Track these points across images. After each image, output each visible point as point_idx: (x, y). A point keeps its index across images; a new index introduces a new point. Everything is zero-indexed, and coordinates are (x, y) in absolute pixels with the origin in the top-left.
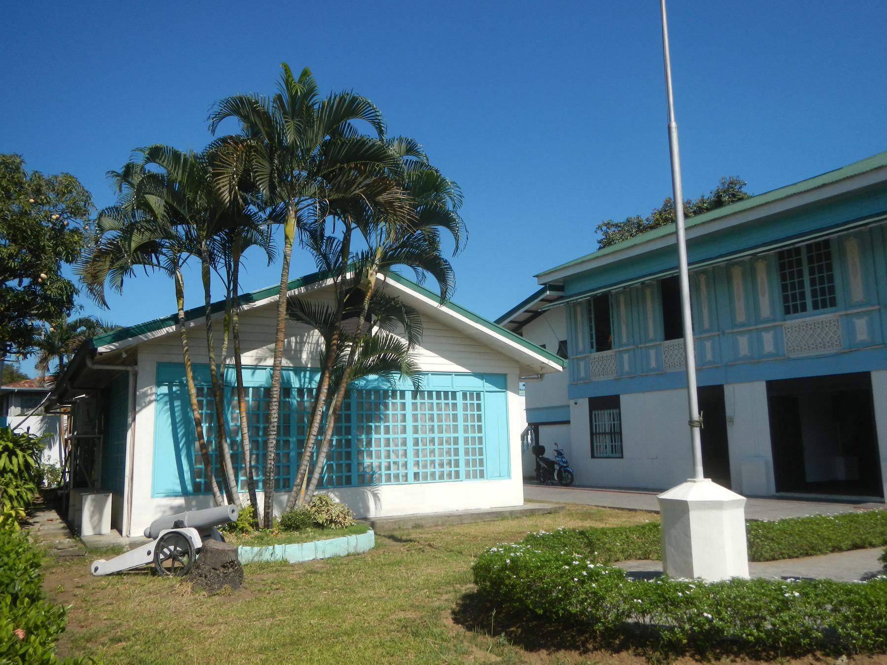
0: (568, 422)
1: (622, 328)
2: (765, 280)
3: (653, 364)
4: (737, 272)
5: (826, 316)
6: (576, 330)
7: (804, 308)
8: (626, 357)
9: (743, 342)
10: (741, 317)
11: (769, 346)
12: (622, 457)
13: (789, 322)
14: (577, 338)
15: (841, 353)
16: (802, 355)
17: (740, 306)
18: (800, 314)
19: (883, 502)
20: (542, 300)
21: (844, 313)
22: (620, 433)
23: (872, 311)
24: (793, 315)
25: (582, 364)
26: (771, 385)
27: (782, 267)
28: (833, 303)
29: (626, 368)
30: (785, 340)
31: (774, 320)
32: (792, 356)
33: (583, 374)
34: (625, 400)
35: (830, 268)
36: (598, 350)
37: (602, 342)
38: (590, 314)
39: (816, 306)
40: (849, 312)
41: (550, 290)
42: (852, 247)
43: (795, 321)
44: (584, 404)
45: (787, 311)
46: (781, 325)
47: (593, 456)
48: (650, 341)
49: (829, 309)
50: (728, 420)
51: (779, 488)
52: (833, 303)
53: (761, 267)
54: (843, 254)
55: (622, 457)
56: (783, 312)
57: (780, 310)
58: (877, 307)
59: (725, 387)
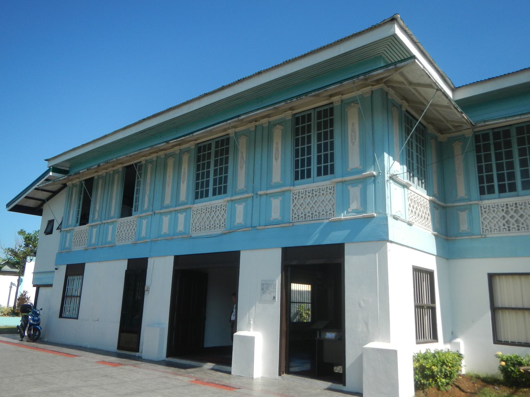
0: (51, 286)
2: (186, 170)
3: (109, 239)
4: (171, 162)
5: (219, 201)
6: (70, 207)
7: (207, 196)
8: (95, 230)
9: (166, 219)
10: (167, 201)
11: (181, 228)
12: (77, 318)
13: (195, 205)
14: (69, 213)
15: (225, 234)
16: (199, 235)
17: (169, 190)
18: (204, 199)
19: (230, 373)
20: (47, 180)
21: (229, 199)
22: (80, 297)
23: (248, 197)
24: (199, 200)
25: (69, 235)
26: (177, 258)
27: (198, 160)
28: (225, 192)
29: (93, 241)
30: (191, 221)
31: (186, 204)
32: (194, 235)
33: (67, 245)
34: (89, 268)
35: (227, 162)
36: (81, 224)
37: (84, 219)
38: (81, 194)
39: (214, 194)
40: (234, 198)
41: (53, 172)
42: (242, 143)
43: (201, 204)
44: (63, 270)
45: (197, 198)
46: (190, 208)
47: (61, 316)
48: (111, 218)
49: (222, 195)
50: (146, 289)
51: (170, 353)
52: (225, 192)
53: (185, 158)
54: (236, 148)
55: (77, 318)
57: (192, 195)
58: (250, 195)
59: (149, 260)
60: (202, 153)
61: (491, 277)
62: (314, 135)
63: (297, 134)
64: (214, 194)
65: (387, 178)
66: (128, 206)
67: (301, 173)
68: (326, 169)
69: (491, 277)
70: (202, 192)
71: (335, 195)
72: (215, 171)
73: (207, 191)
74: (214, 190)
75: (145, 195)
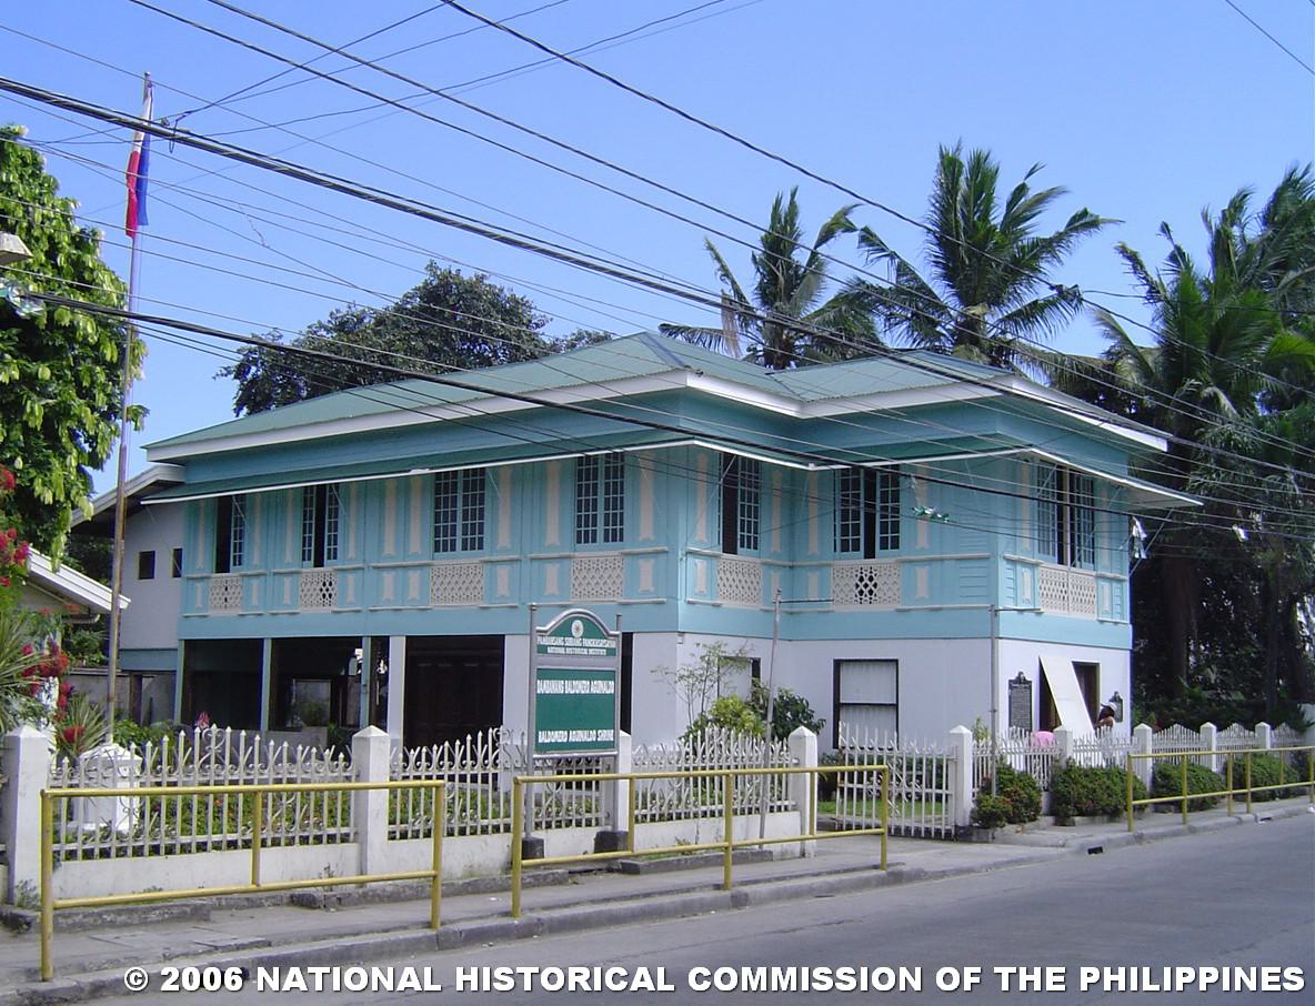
1: (255, 550)
27: (437, 491)
52: (481, 547)
56: (432, 548)
60: (443, 487)
61: (838, 664)
62: (601, 481)
63: (580, 480)
64: (465, 548)
65: (680, 556)
66: (318, 550)
67: (584, 537)
68: (615, 536)
69: (838, 664)
70: (445, 542)
71: (624, 571)
72: (465, 513)
73: (453, 543)
74: (465, 542)
75: (350, 542)
